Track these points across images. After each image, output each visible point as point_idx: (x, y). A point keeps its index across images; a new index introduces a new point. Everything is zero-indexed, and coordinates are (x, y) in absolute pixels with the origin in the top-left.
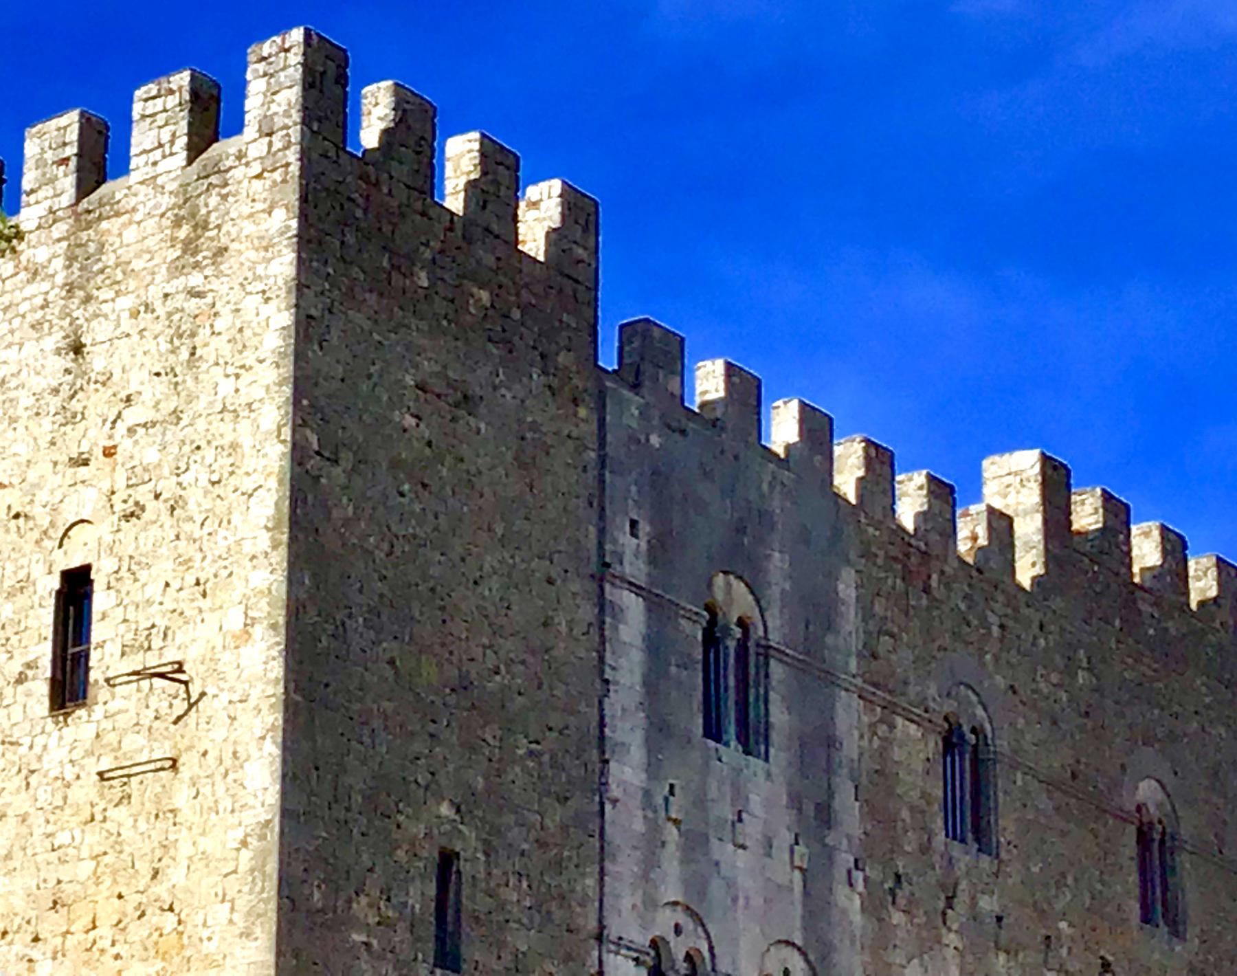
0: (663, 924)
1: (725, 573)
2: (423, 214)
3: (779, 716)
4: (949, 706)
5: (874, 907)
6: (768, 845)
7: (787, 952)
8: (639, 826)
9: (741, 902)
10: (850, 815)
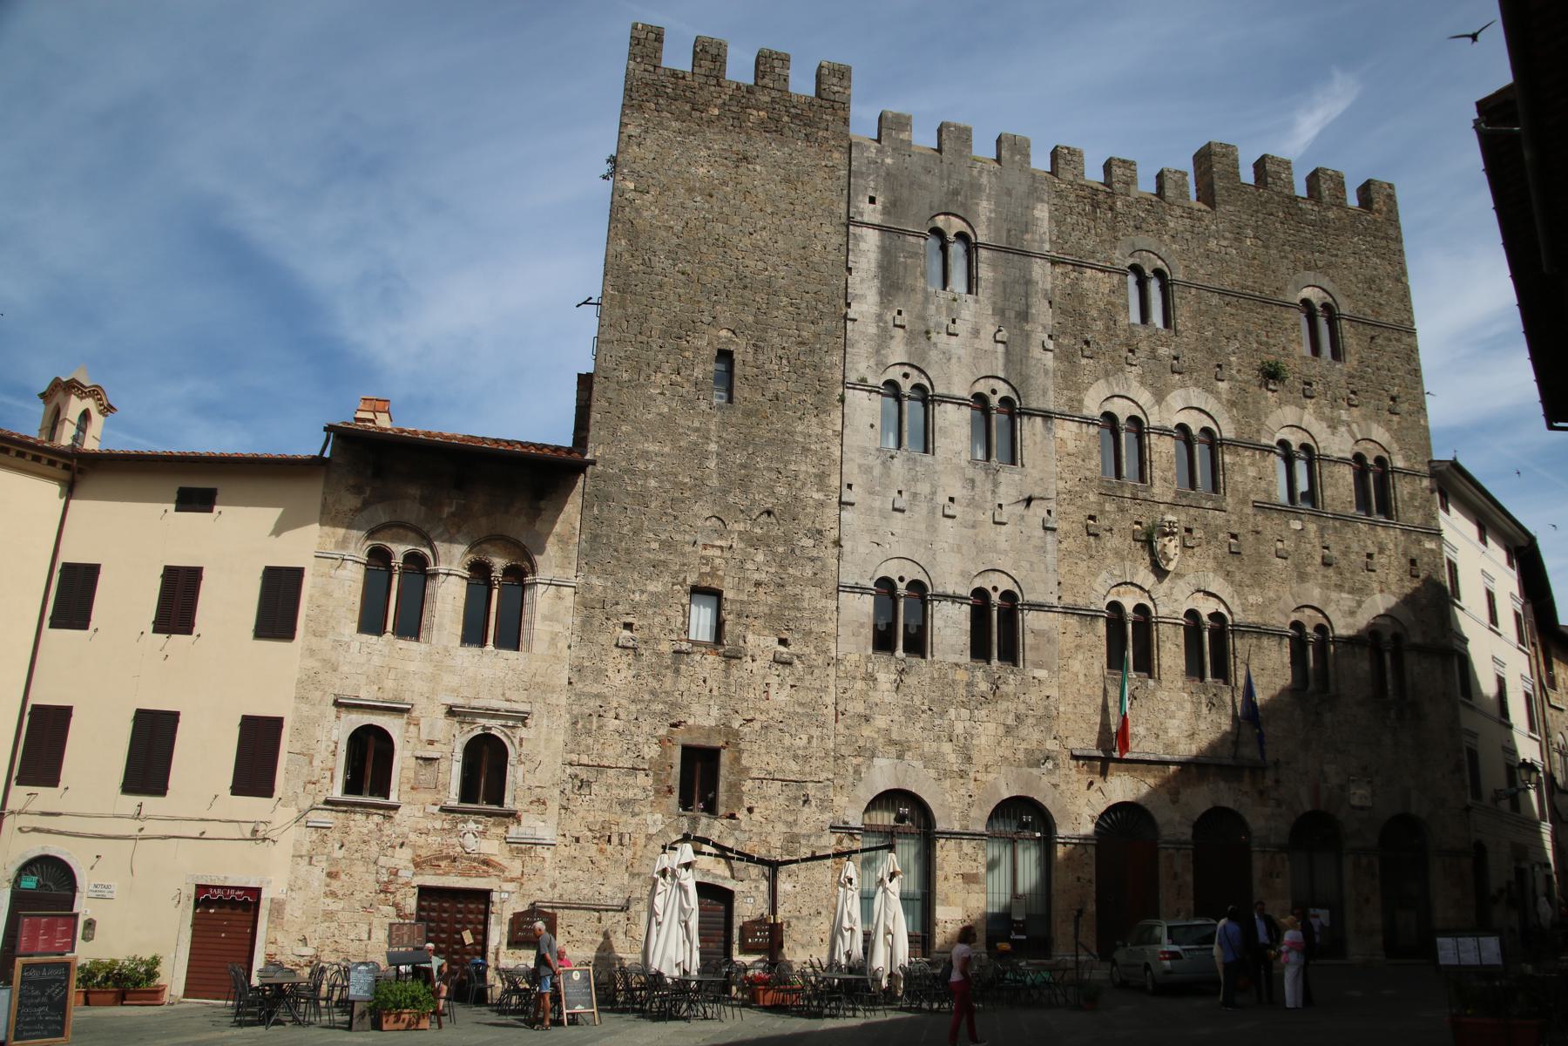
0: (895, 374)
1: (945, 214)
2: (719, 85)
3: (985, 272)
4: (1130, 261)
5: (1066, 356)
6: (976, 333)
7: (992, 381)
8: (872, 330)
9: (954, 361)
10: (1043, 315)
